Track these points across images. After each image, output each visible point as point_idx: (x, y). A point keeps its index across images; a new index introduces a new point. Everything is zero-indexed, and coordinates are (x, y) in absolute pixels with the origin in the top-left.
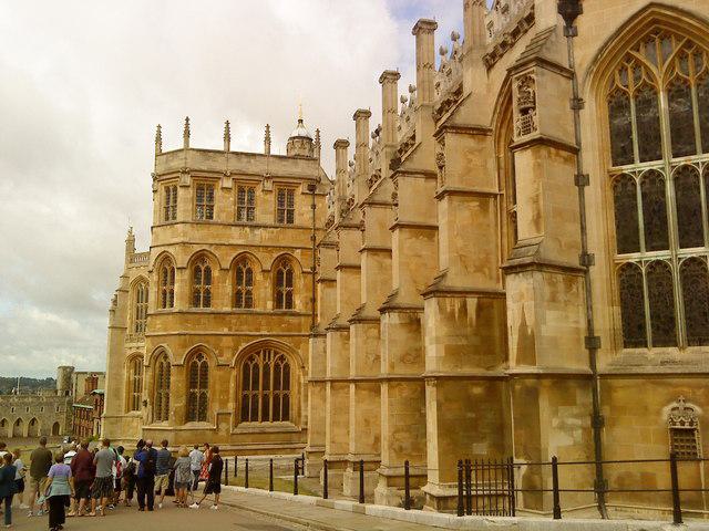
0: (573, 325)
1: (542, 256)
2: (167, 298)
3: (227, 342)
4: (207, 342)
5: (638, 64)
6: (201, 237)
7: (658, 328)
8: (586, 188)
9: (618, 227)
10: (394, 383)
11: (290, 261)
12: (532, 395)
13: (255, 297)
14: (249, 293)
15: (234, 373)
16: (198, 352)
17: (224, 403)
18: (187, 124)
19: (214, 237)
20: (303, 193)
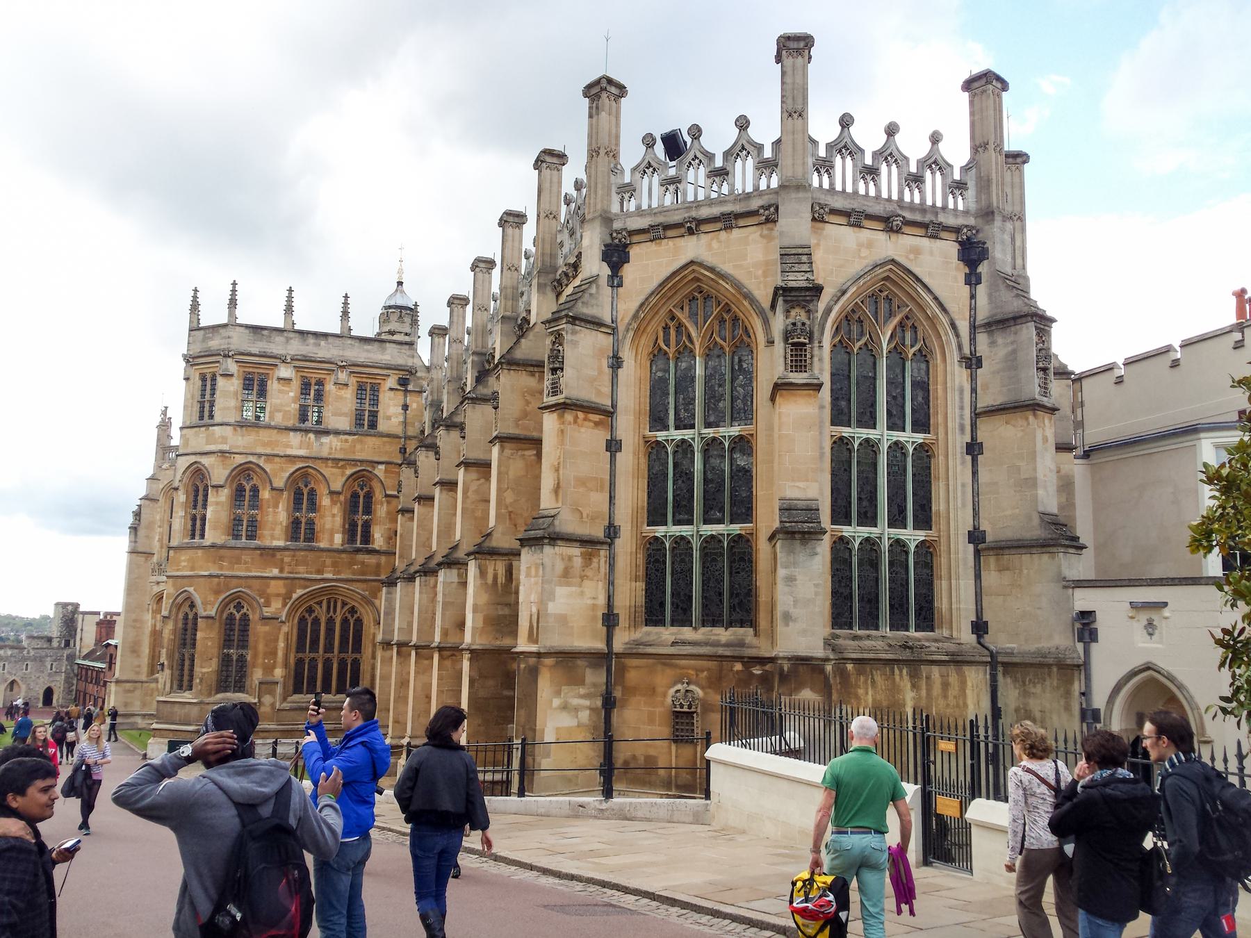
0: (590, 602)
1: (557, 529)
2: (197, 526)
4: (249, 587)
5: (680, 326)
7: (678, 606)
8: (618, 454)
10: (446, 653)
11: (370, 480)
12: (534, 672)
13: (317, 528)
14: (311, 523)
15: (285, 629)
16: (237, 601)
17: (269, 669)
18: (234, 291)
19: (265, 445)
20: (391, 389)
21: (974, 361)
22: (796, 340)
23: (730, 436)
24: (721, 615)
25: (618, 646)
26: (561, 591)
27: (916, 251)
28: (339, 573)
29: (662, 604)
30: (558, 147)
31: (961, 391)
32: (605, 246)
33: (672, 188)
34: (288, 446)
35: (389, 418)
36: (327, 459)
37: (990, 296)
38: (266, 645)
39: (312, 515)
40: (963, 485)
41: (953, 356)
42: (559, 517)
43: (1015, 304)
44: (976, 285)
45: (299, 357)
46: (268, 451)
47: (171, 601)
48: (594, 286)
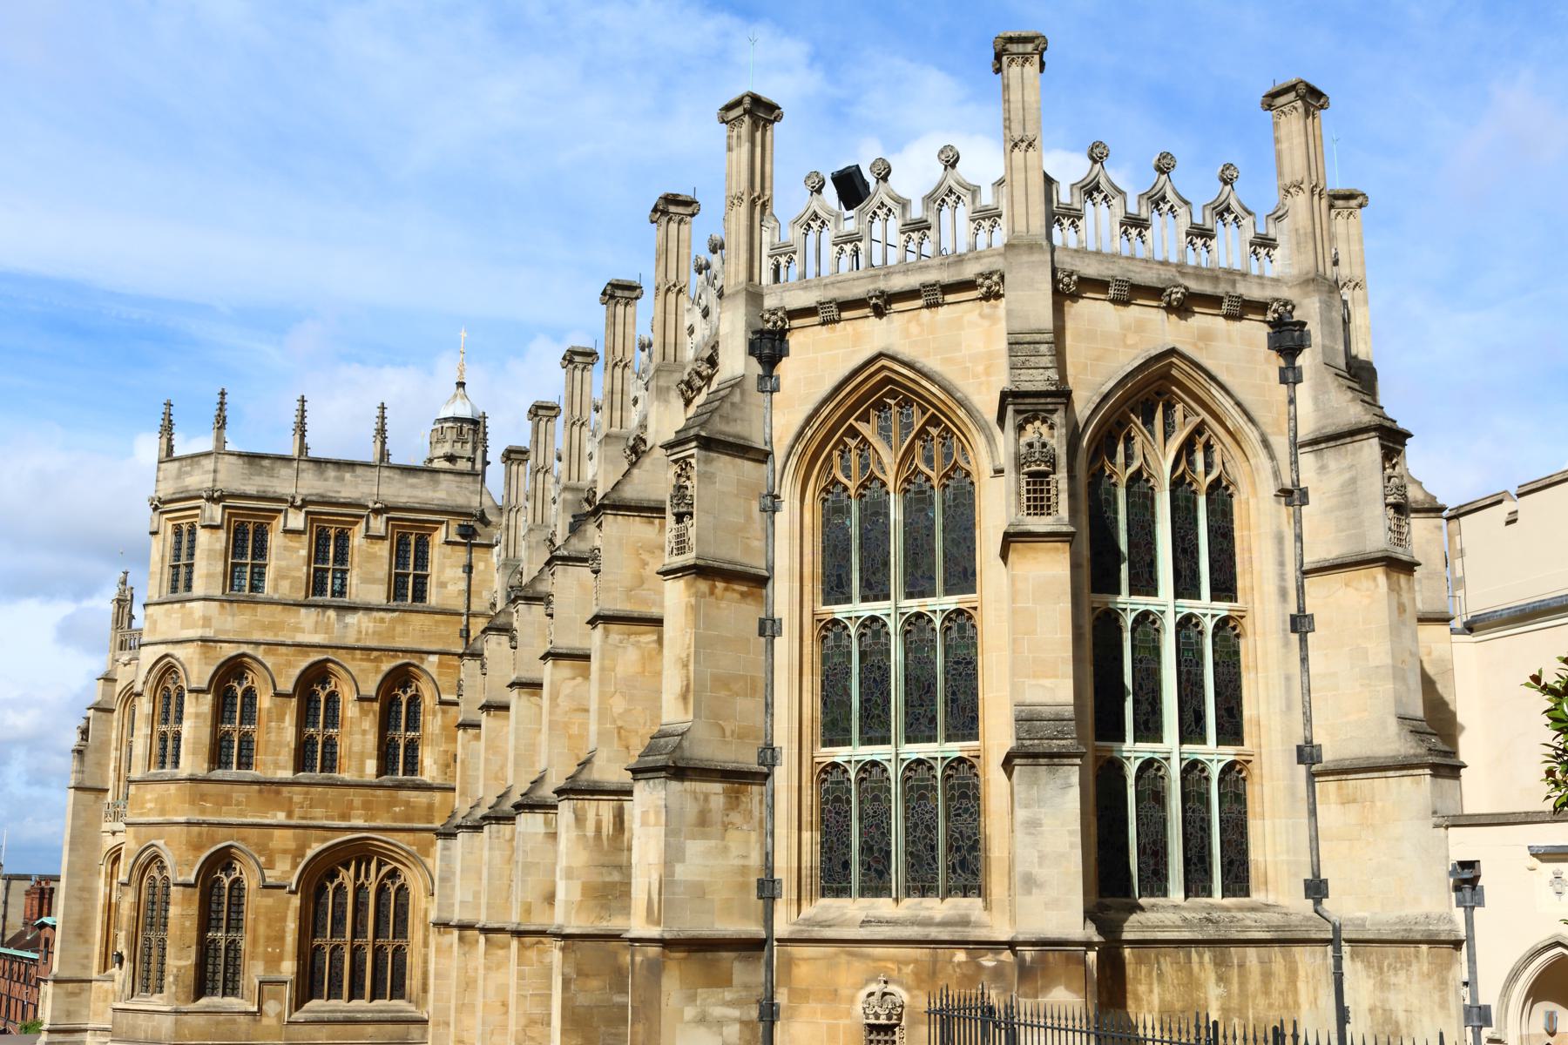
1: (687, 754)
2: (166, 750)
3: (283, 840)
4: (243, 840)
6: (235, 624)
7: (869, 869)
9: (825, 704)
10: (528, 940)
13: (342, 749)
14: (330, 743)
16: (222, 860)
19: (265, 628)
20: (448, 543)
21: (1296, 495)
22: (1034, 468)
23: (943, 611)
24: (934, 879)
25: (781, 928)
26: (695, 848)
27: (1206, 337)
28: (372, 818)
29: (846, 865)
30: (685, 191)
31: (1280, 539)
32: (754, 333)
33: (848, 248)
34: (297, 629)
35: (443, 585)
36: (354, 649)
37: (1316, 400)
38: (269, 926)
39: (331, 731)
40: (1288, 678)
41: (1268, 488)
42: (689, 735)
43: (1352, 411)
44: (1295, 384)
45: (314, 498)
46: (270, 638)
47: (132, 860)
48: (737, 391)
